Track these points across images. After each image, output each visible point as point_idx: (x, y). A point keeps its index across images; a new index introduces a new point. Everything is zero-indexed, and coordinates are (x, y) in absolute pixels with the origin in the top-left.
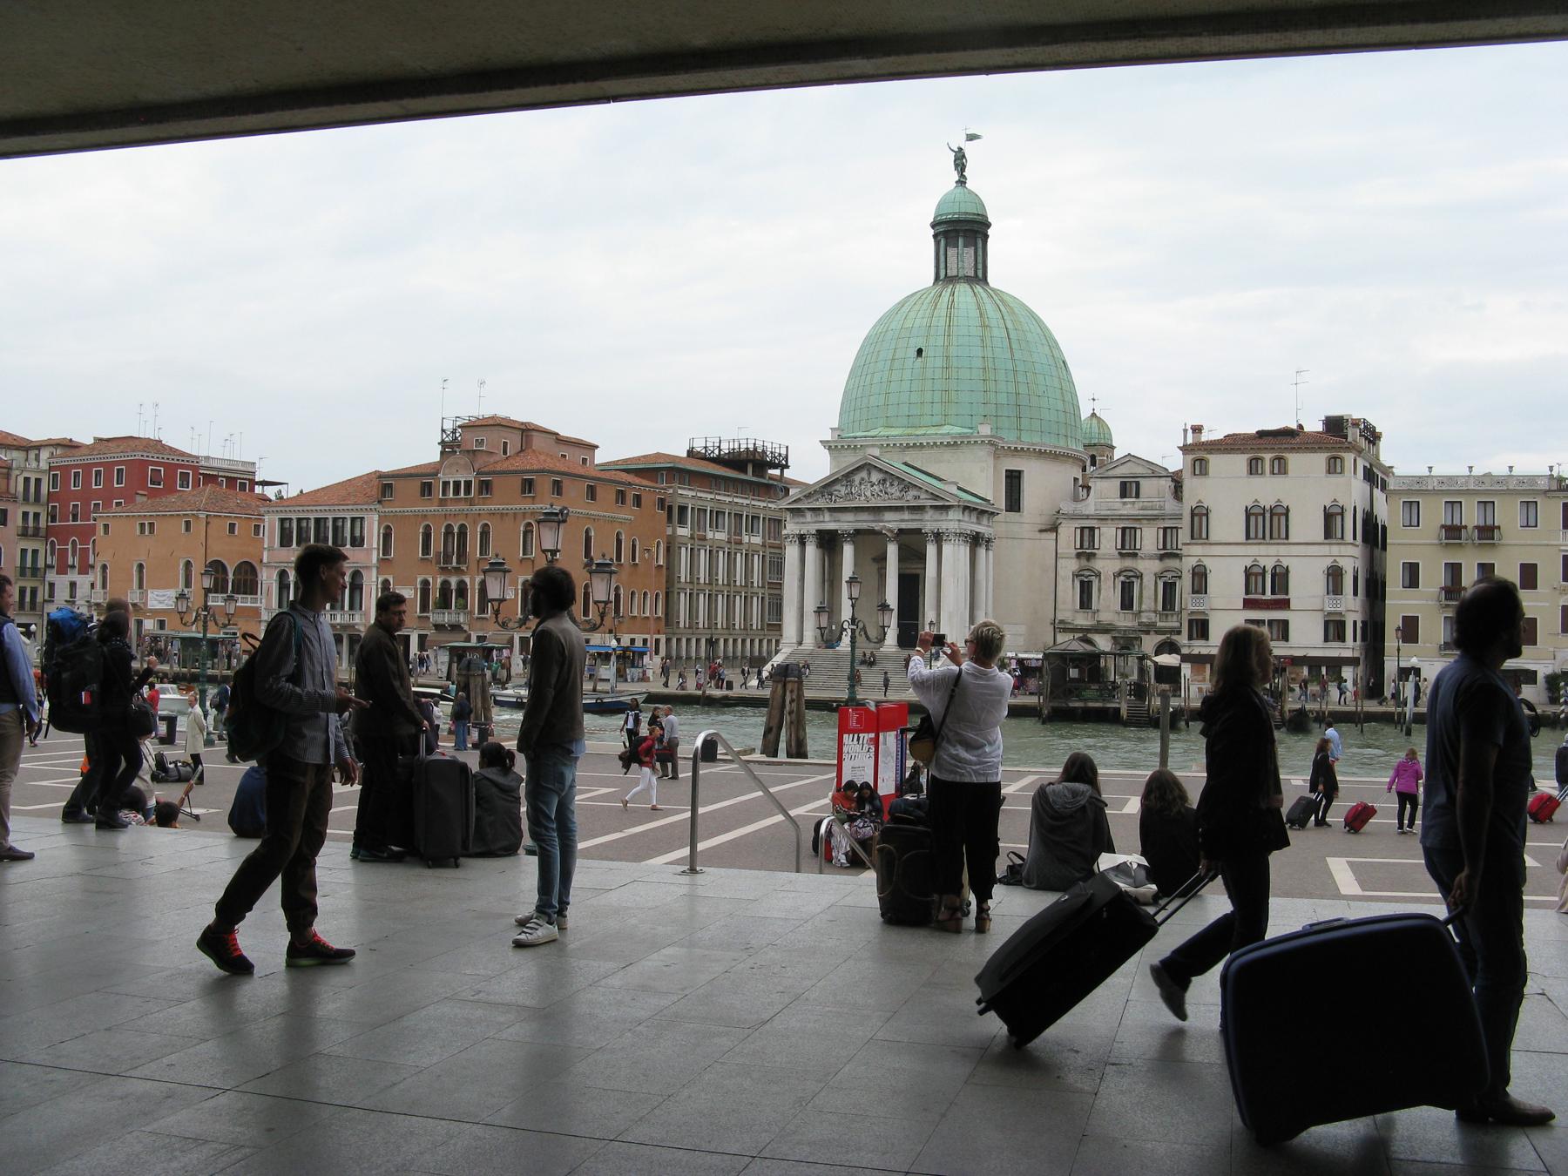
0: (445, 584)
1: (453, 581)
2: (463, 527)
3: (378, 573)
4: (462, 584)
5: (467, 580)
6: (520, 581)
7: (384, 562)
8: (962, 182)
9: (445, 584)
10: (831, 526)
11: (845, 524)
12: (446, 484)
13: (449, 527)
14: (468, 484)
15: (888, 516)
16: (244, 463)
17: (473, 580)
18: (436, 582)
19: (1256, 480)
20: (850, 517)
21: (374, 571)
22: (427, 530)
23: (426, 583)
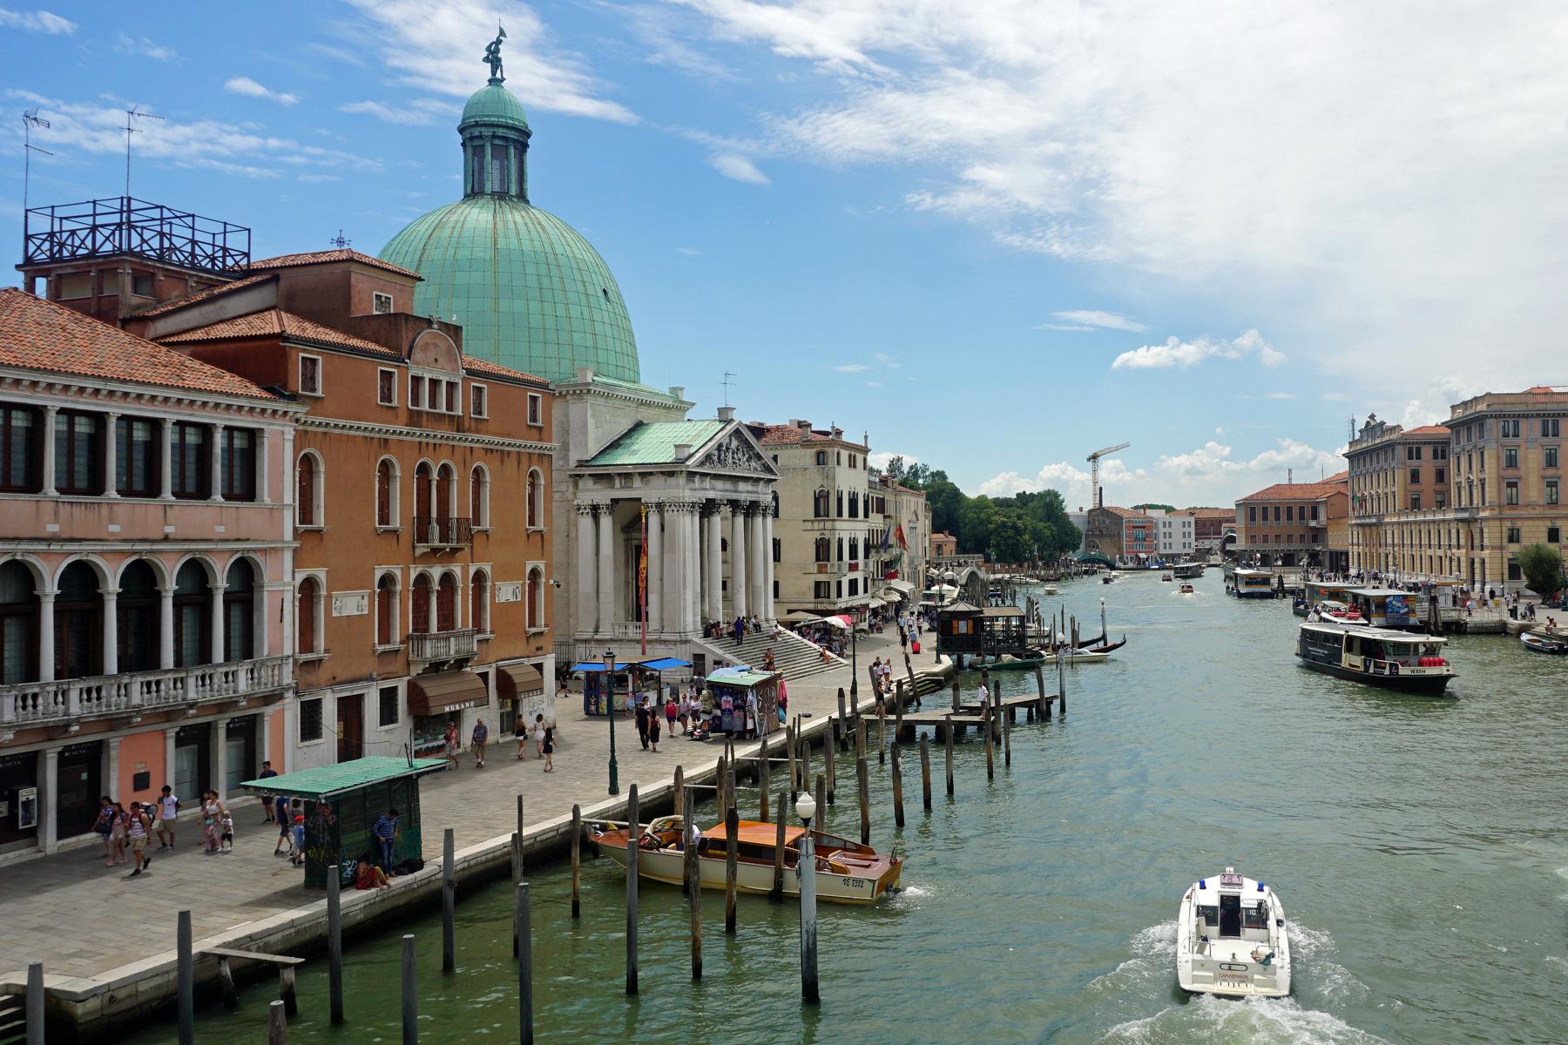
0: (423, 580)
1: (436, 572)
2: (445, 470)
3: (297, 564)
4: (447, 579)
5: (457, 570)
6: (528, 570)
7: (308, 534)
8: (494, 81)
9: (423, 580)
10: (711, 495)
11: (717, 491)
12: (417, 380)
13: (424, 469)
14: (451, 386)
15: (742, 486)
16: (314, 255)
17: (465, 570)
18: (405, 576)
19: (852, 471)
20: (719, 484)
21: (288, 557)
22: (386, 467)
23: (387, 582)
